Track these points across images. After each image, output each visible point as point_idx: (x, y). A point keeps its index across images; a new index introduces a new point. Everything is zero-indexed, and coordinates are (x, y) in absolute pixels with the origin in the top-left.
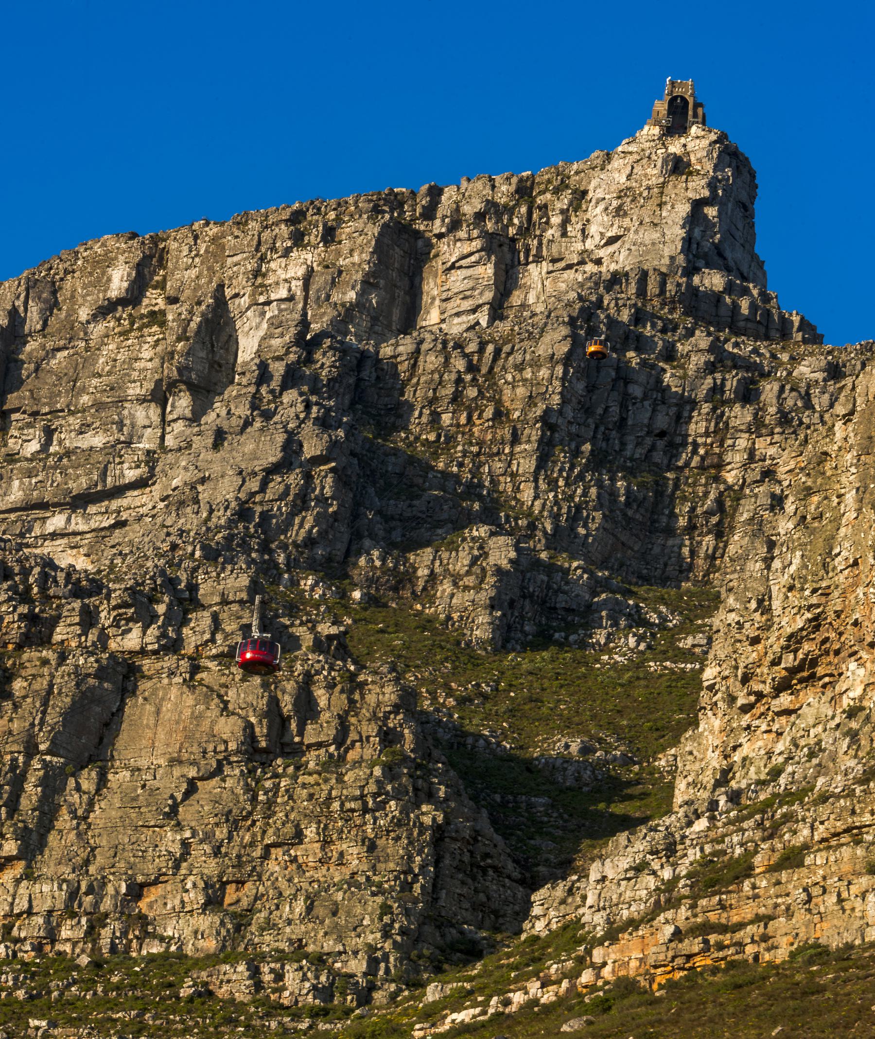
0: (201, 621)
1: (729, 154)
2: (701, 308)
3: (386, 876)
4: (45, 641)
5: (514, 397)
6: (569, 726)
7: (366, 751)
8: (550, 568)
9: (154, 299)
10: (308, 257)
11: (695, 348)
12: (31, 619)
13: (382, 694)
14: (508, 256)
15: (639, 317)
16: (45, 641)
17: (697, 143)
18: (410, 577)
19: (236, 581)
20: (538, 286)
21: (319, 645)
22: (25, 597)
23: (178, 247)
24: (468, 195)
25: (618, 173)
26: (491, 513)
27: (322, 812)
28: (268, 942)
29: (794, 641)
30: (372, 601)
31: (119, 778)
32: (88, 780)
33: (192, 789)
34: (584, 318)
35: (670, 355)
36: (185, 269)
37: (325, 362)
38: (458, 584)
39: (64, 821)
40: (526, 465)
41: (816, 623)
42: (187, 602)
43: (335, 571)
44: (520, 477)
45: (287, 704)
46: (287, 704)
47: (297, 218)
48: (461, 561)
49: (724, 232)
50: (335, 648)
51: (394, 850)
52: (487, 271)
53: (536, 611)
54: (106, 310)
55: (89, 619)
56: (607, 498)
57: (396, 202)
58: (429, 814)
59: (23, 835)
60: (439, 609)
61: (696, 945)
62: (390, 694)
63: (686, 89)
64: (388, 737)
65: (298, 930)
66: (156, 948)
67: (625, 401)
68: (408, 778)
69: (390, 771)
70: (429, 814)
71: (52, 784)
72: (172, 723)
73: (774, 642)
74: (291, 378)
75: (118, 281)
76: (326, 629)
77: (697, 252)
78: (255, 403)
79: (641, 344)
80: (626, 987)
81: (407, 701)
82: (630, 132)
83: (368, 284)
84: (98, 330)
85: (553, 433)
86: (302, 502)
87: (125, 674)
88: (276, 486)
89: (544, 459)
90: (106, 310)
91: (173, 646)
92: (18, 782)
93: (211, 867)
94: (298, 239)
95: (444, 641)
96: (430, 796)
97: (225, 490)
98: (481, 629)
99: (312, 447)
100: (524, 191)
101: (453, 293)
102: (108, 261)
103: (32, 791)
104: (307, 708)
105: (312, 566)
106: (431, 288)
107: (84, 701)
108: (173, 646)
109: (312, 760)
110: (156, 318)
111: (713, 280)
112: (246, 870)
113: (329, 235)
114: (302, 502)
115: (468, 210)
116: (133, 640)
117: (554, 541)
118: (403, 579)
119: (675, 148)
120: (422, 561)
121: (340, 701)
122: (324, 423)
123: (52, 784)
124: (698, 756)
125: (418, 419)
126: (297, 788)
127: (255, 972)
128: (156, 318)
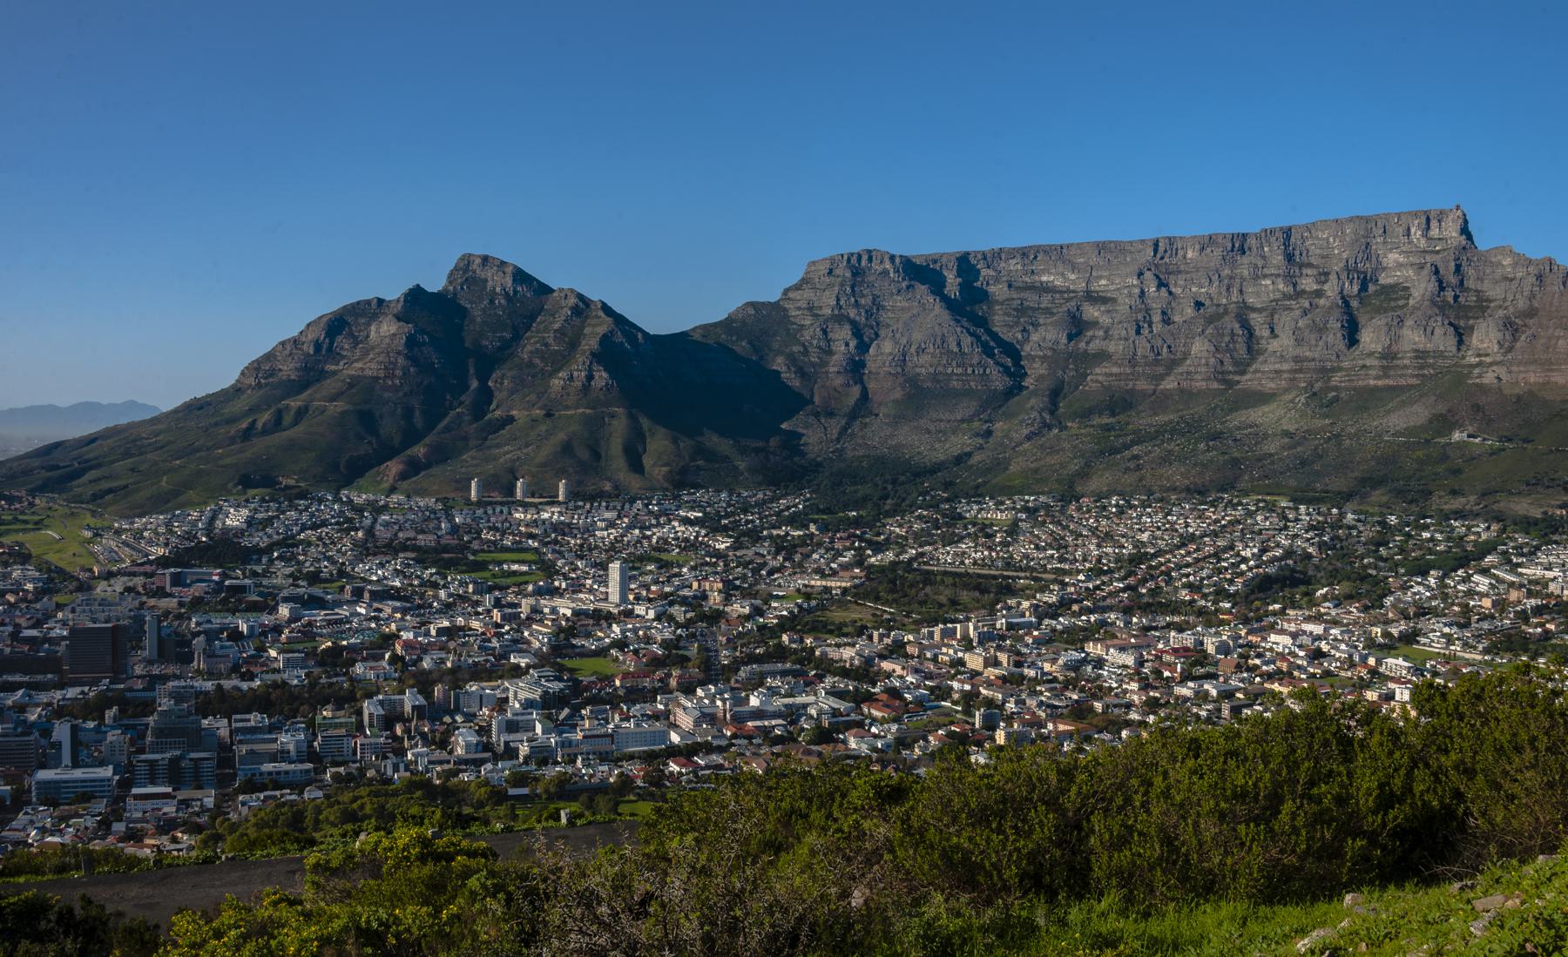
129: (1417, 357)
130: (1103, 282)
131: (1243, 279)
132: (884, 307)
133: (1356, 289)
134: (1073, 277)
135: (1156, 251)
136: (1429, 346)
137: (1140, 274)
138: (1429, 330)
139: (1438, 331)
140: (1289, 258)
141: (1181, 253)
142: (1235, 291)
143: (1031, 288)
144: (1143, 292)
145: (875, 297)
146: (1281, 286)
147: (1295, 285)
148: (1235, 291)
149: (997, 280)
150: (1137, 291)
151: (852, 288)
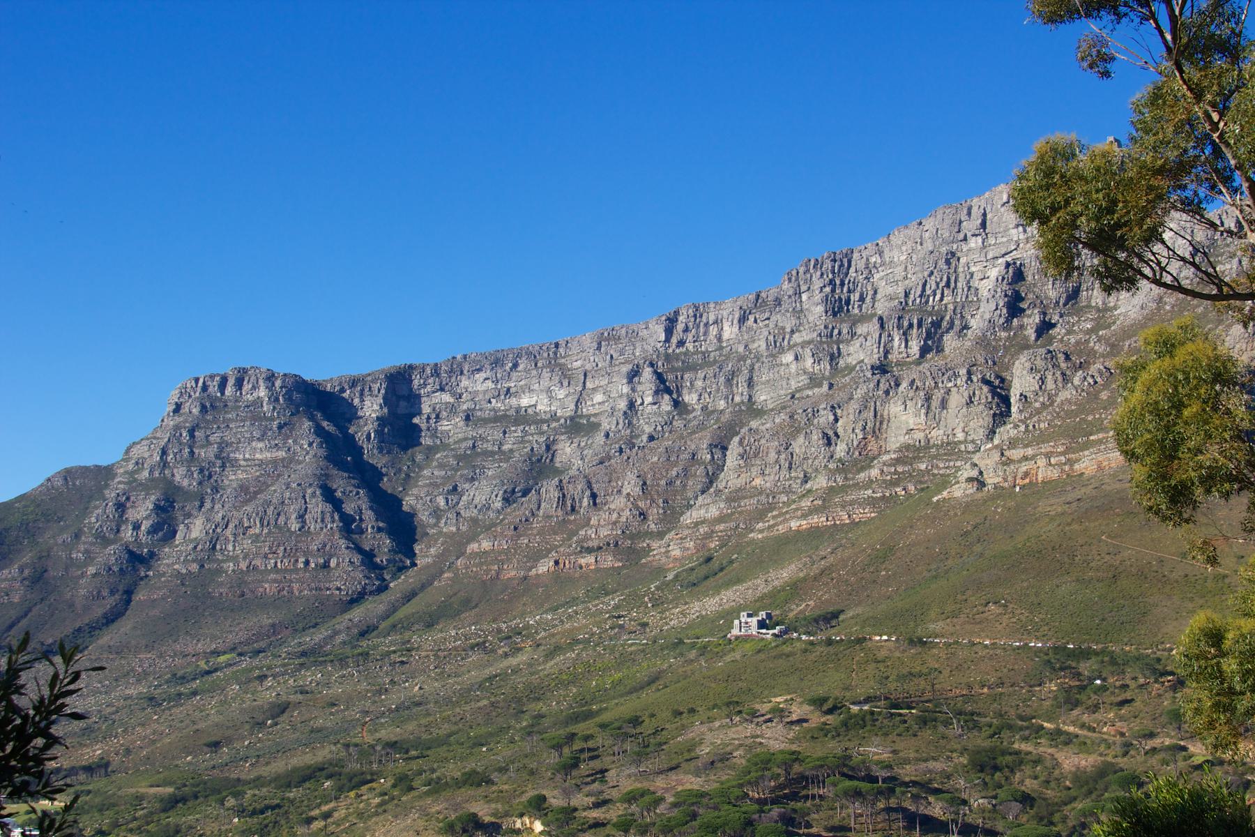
102: (1001, 192)
116: (950, 385)
129: (898, 461)
130: (599, 398)
131: (758, 358)
132: (235, 464)
133: (915, 347)
134: (561, 394)
135: (669, 332)
136: (937, 435)
137: (633, 375)
138: (938, 396)
139: (956, 400)
140: (837, 308)
141: (713, 330)
142: (741, 389)
143: (500, 419)
144: (631, 405)
145: (223, 445)
146: (809, 361)
147: (833, 358)
148: (741, 389)
149: (452, 409)
150: (622, 405)
151: (192, 433)
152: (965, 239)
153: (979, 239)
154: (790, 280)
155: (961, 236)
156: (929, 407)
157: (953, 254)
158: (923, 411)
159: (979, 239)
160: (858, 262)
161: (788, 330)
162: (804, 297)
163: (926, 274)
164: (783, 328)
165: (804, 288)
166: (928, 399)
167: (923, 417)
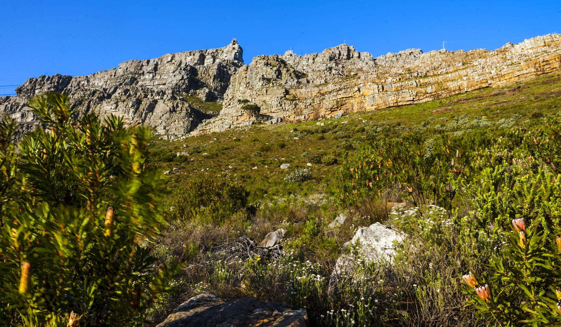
0: (166, 96)
1: (240, 47)
2: (234, 64)
3: (185, 126)
4: (147, 97)
5: (211, 73)
6: (212, 110)
7: (184, 112)
8: (213, 93)
9: (173, 61)
10: (191, 57)
11: (233, 69)
12: (145, 95)
13: (186, 105)
14: (214, 58)
15: (227, 65)
16: (147, 97)
17: (236, 46)
18: (196, 93)
19: (170, 91)
20: (217, 61)
21: (180, 99)
22: (145, 92)
23: (176, 55)
24: (210, 51)
25: (227, 49)
26: (207, 87)
27: (178, 119)
28: (170, 133)
29: (230, 99)
30: (191, 95)
31: (154, 114)
32: (151, 114)
33: (163, 115)
34: (220, 65)
35: (230, 69)
36: (177, 58)
37: (189, 68)
38: (202, 94)
39: (147, 118)
40: (212, 81)
41: (233, 97)
42: (164, 93)
43: (187, 92)
44: (211, 83)
45: (175, 106)
46: (175, 106)
47: (190, 52)
48: (202, 91)
49: (239, 57)
50: (183, 100)
51: (186, 123)
52: (212, 60)
53: (211, 97)
54: (168, 62)
55: (152, 95)
56: (221, 85)
57: (202, 51)
58: (191, 119)
59: (142, 120)
60: (199, 97)
61: (201, 132)
62: (187, 105)
63: (235, 40)
64: (187, 110)
65: (174, 132)
66: (157, 134)
67: (224, 74)
68: (189, 115)
69: (186, 114)
70: (191, 119)
71: (146, 114)
72: (161, 107)
73: (229, 99)
74: (184, 69)
75: (169, 59)
76: (181, 97)
77: (235, 58)
78: (179, 72)
79: (226, 68)
80: (194, 136)
81: (189, 106)
82: (229, 44)
83: (198, 61)
84: (167, 64)
85: (215, 78)
86: (184, 84)
87: (156, 102)
88: (181, 82)
89: (214, 80)
90: (168, 62)
91: (162, 99)
92: (142, 114)
93: (165, 124)
94: (190, 55)
95: (200, 101)
96: (191, 117)
97: (175, 82)
98: (204, 99)
99: (185, 77)
100: (217, 51)
101: (208, 61)
102: (168, 57)
103: (144, 115)
104: (177, 106)
105: (185, 91)
106: (206, 61)
107: (150, 105)
108: (162, 99)
109: (178, 112)
110: (174, 63)
111: (236, 61)
112: (169, 125)
113: (194, 55)
114: (184, 84)
115: (210, 52)
116: (157, 98)
117: (214, 90)
118: (195, 93)
119: (234, 46)
120: (198, 91)
121: (181, 106)
122: (187, 75)
123: (146, 114)
124: (222, 112)
125: (199, 75)
126: (176, 116)
127: (168, 137)
128: (174, 63)
152: (143, 74)
153: (151, 75)
154: (31, 82)
155: (141, 72)
156: (137, 109)
157: (136, 79)
158: (132, 110)
159: (151, 75)
160: (74, 83)
161: (22, 104)
162: (37, 91)
163: (118, 84)
164: (18, 104)
165: (38, 87)
166: (138, 102)
167: (131, 113)
